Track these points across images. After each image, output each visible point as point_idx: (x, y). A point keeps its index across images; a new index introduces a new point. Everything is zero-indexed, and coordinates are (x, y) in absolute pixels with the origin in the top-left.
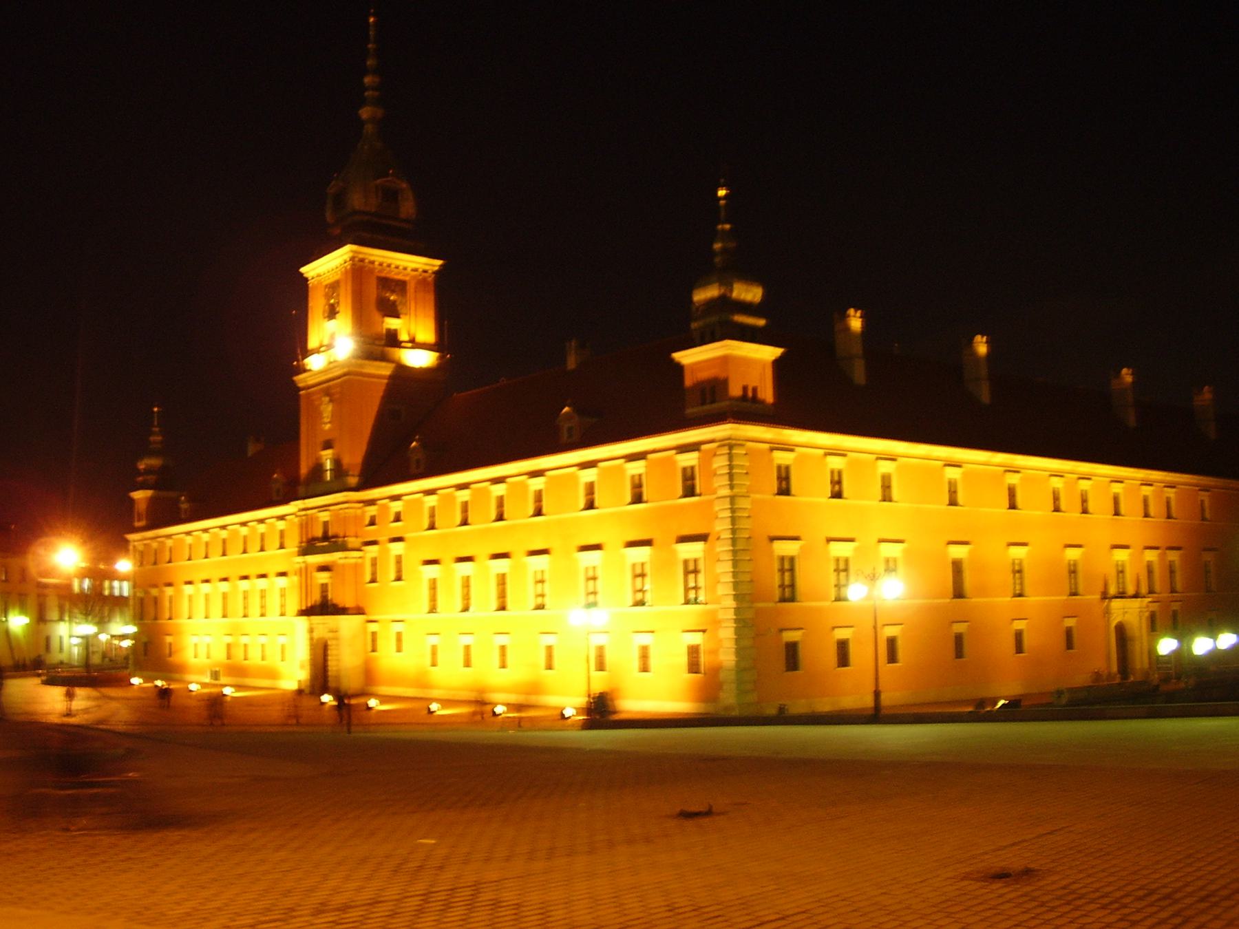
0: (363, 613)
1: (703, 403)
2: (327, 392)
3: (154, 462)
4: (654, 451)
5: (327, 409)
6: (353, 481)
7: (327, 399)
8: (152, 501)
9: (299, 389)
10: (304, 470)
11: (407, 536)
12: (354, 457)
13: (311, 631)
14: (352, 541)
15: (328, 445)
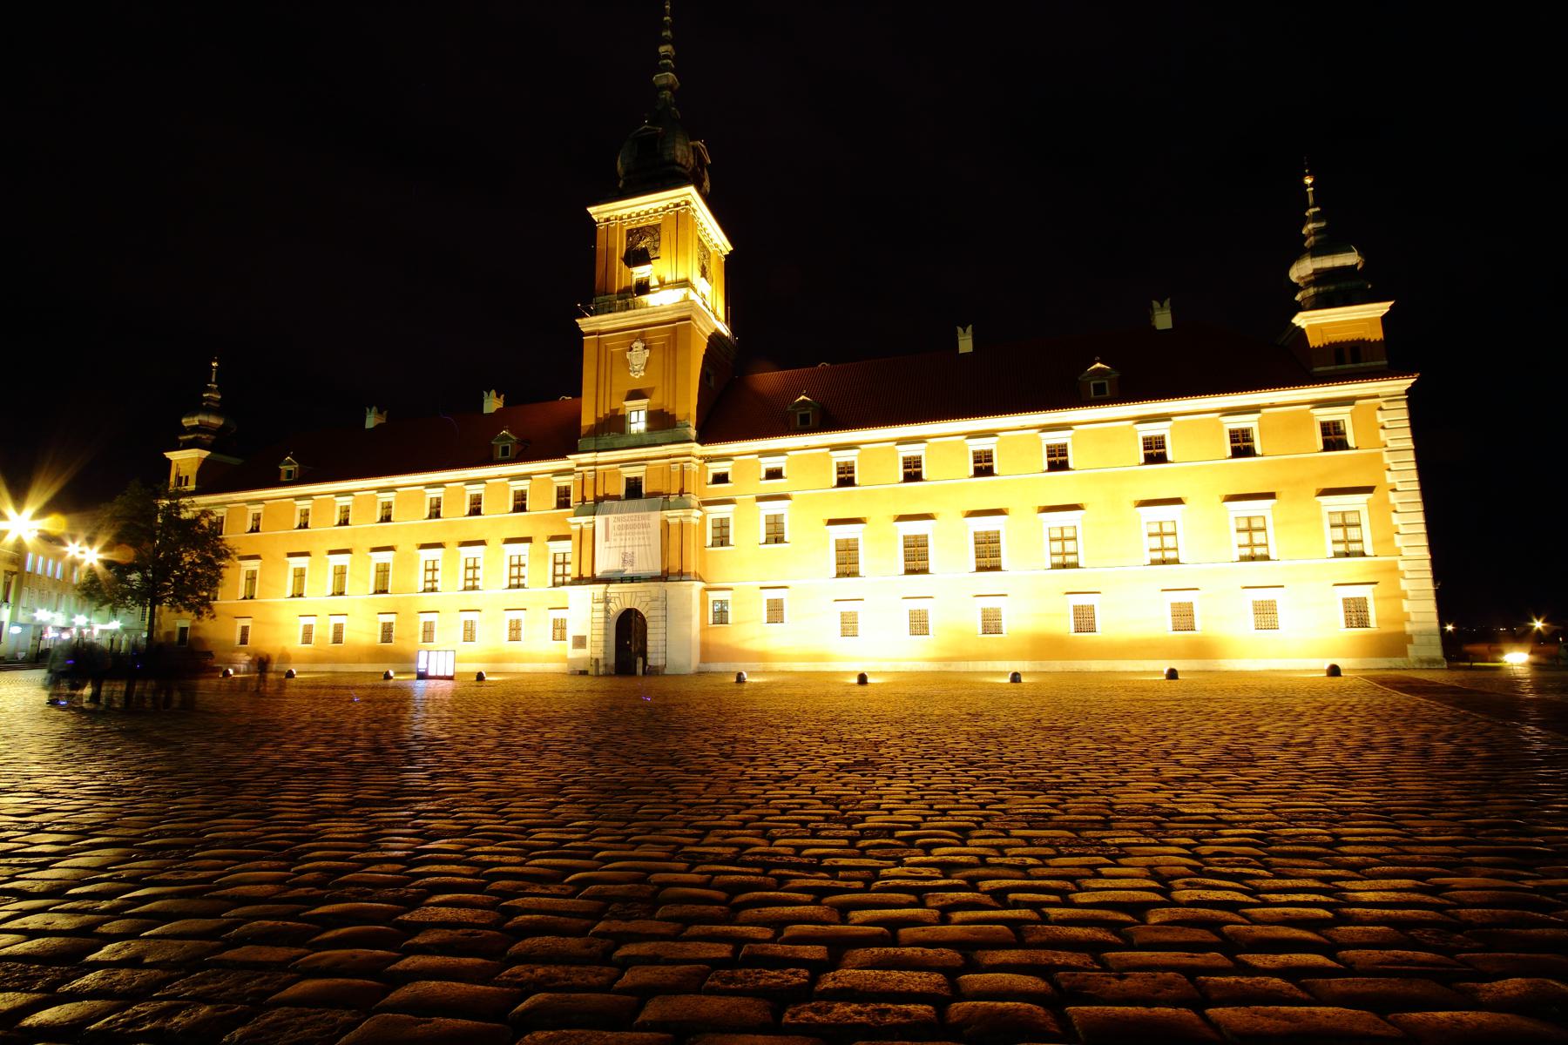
0: (701, 580)
1: (1340, 361)
2: (641, 337)
3: (214, 421)
4: (1272, 406)
5: (638, 356)
6: (693, 433)
7: (638, 345)
8: (205, 466)
9: (583, 334)
10: (587, 420)
11: (794, 494)
12: (687, 407)
13: (607, 601)
14: (694, 501)
15: (635, 395)
